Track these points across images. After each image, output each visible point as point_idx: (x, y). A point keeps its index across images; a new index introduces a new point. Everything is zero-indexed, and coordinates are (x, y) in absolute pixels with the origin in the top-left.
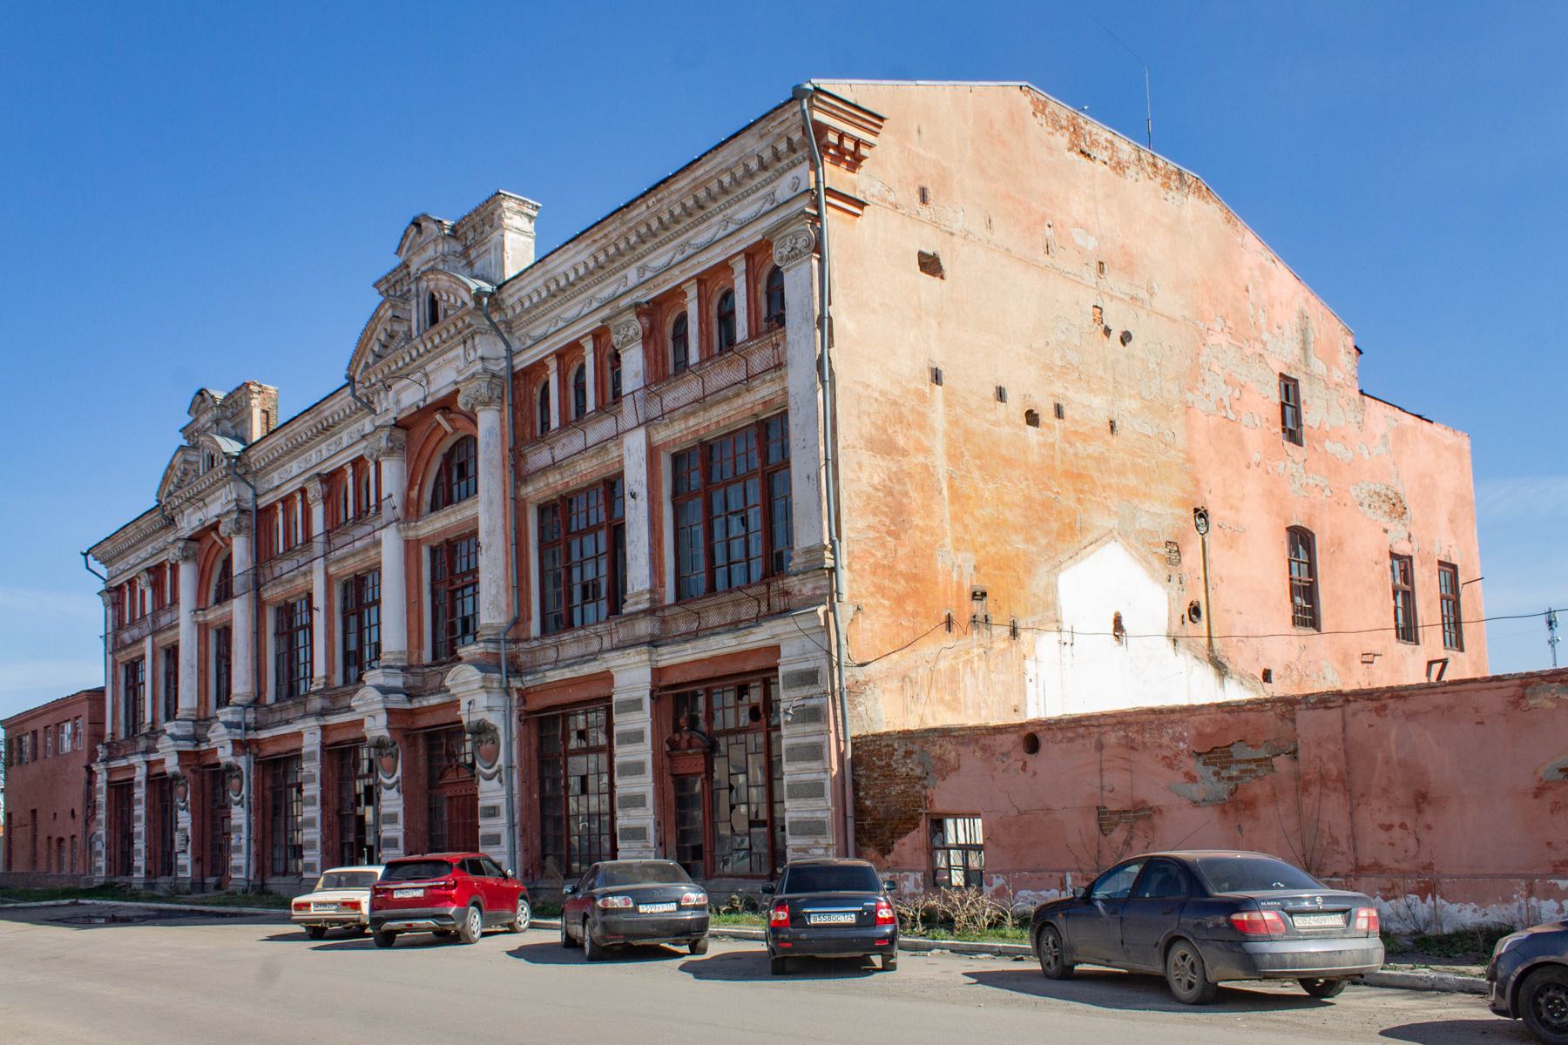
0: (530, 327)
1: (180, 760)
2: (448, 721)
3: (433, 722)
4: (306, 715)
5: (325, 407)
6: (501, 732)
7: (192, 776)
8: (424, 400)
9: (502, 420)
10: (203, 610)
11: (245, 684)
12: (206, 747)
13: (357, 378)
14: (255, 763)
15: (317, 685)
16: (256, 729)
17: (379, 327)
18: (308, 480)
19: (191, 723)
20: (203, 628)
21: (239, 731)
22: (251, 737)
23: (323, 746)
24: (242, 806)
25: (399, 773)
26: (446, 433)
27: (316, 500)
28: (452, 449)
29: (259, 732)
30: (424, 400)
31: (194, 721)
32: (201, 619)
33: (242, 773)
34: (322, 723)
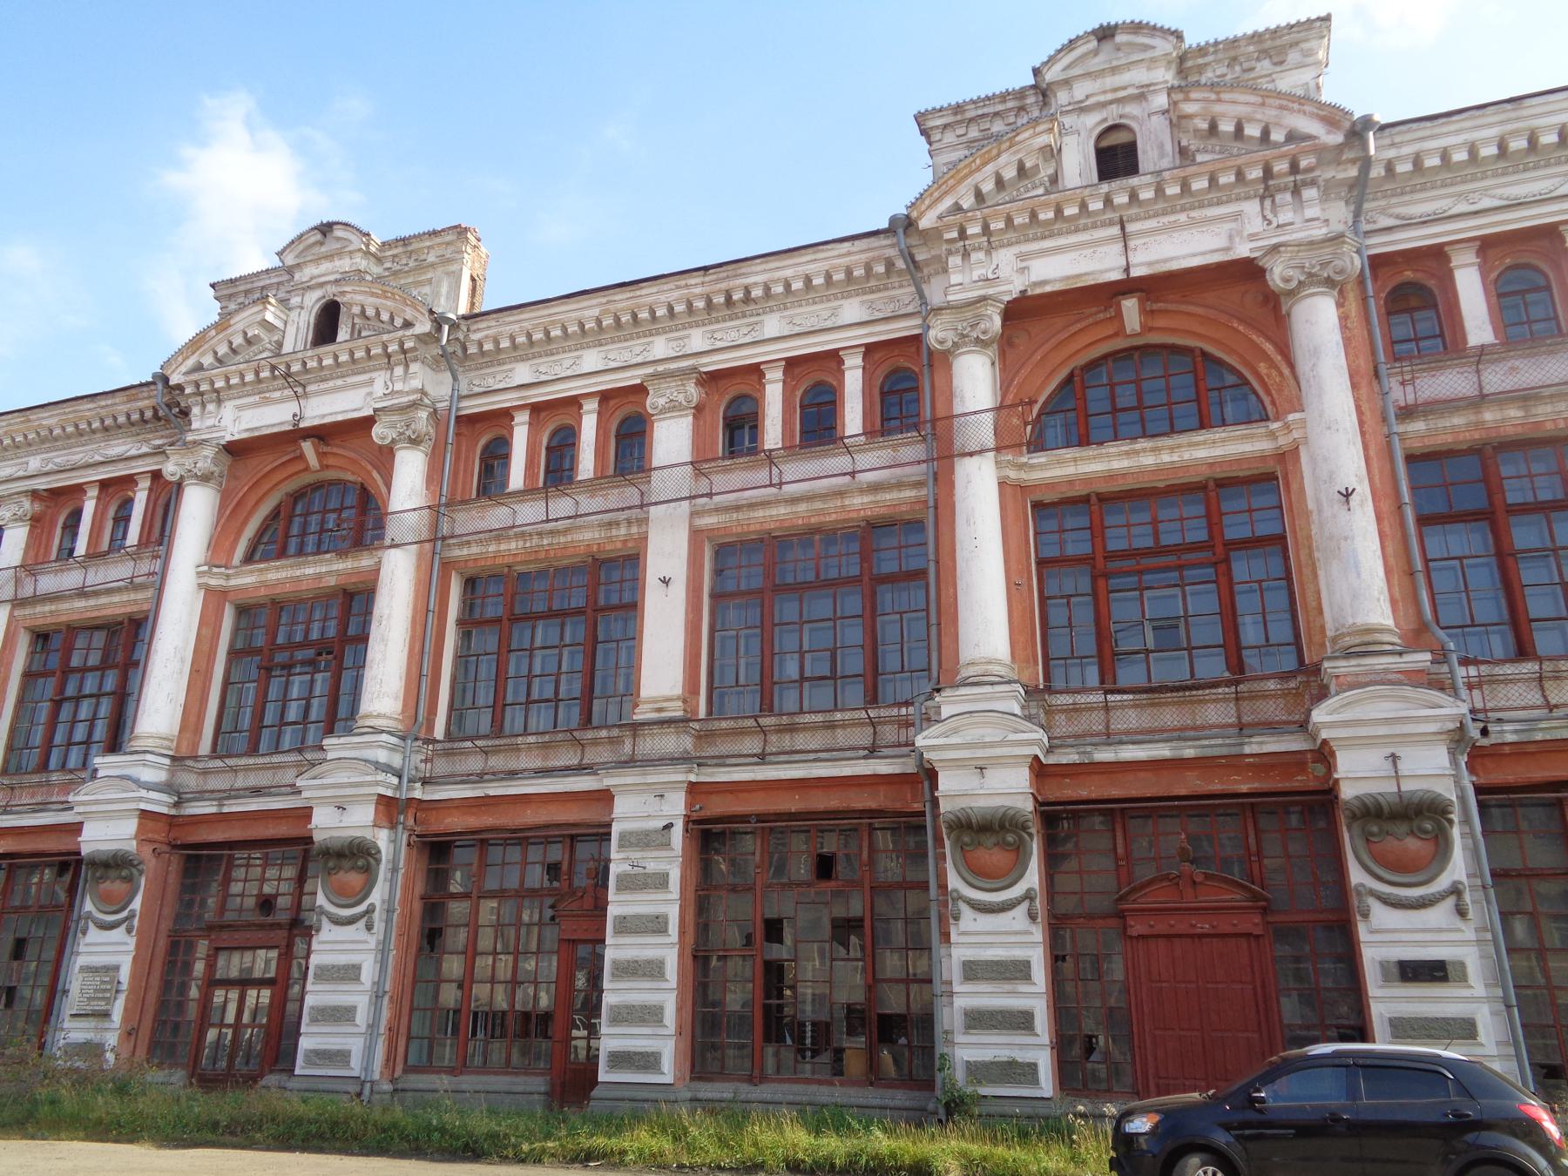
0: (1394, 200)
1: (141, 828)
2: (1183, 792)
3: (1116, 793)
4: (630, 762)
5: (759, 268)
6: (1455, 817)
7: (154, 861)
8: (1127, 270)
9: (1344, 319)
10: (226, 568)
11: (396, 698)
12: (213, 810)
13: (924, 223)
14: (409, 844)
15: (660, 710)
16: (426, 782)
17: (1004, 158)
18: (657, 376)
19: (167, 761)
20: (214, 598)
21: (395, 780)
22: (418, 793)
23: (689, 821)
24: (369, 927)
25: (1032, 877)
26: (1120, 332)
27: (673, 408)
28: (1093, 365)
29: (428, 788)
30: (1127, 270)
31: (173, 758)
32: (213, 582)
33: (378, 861)
34: (693, 778)
